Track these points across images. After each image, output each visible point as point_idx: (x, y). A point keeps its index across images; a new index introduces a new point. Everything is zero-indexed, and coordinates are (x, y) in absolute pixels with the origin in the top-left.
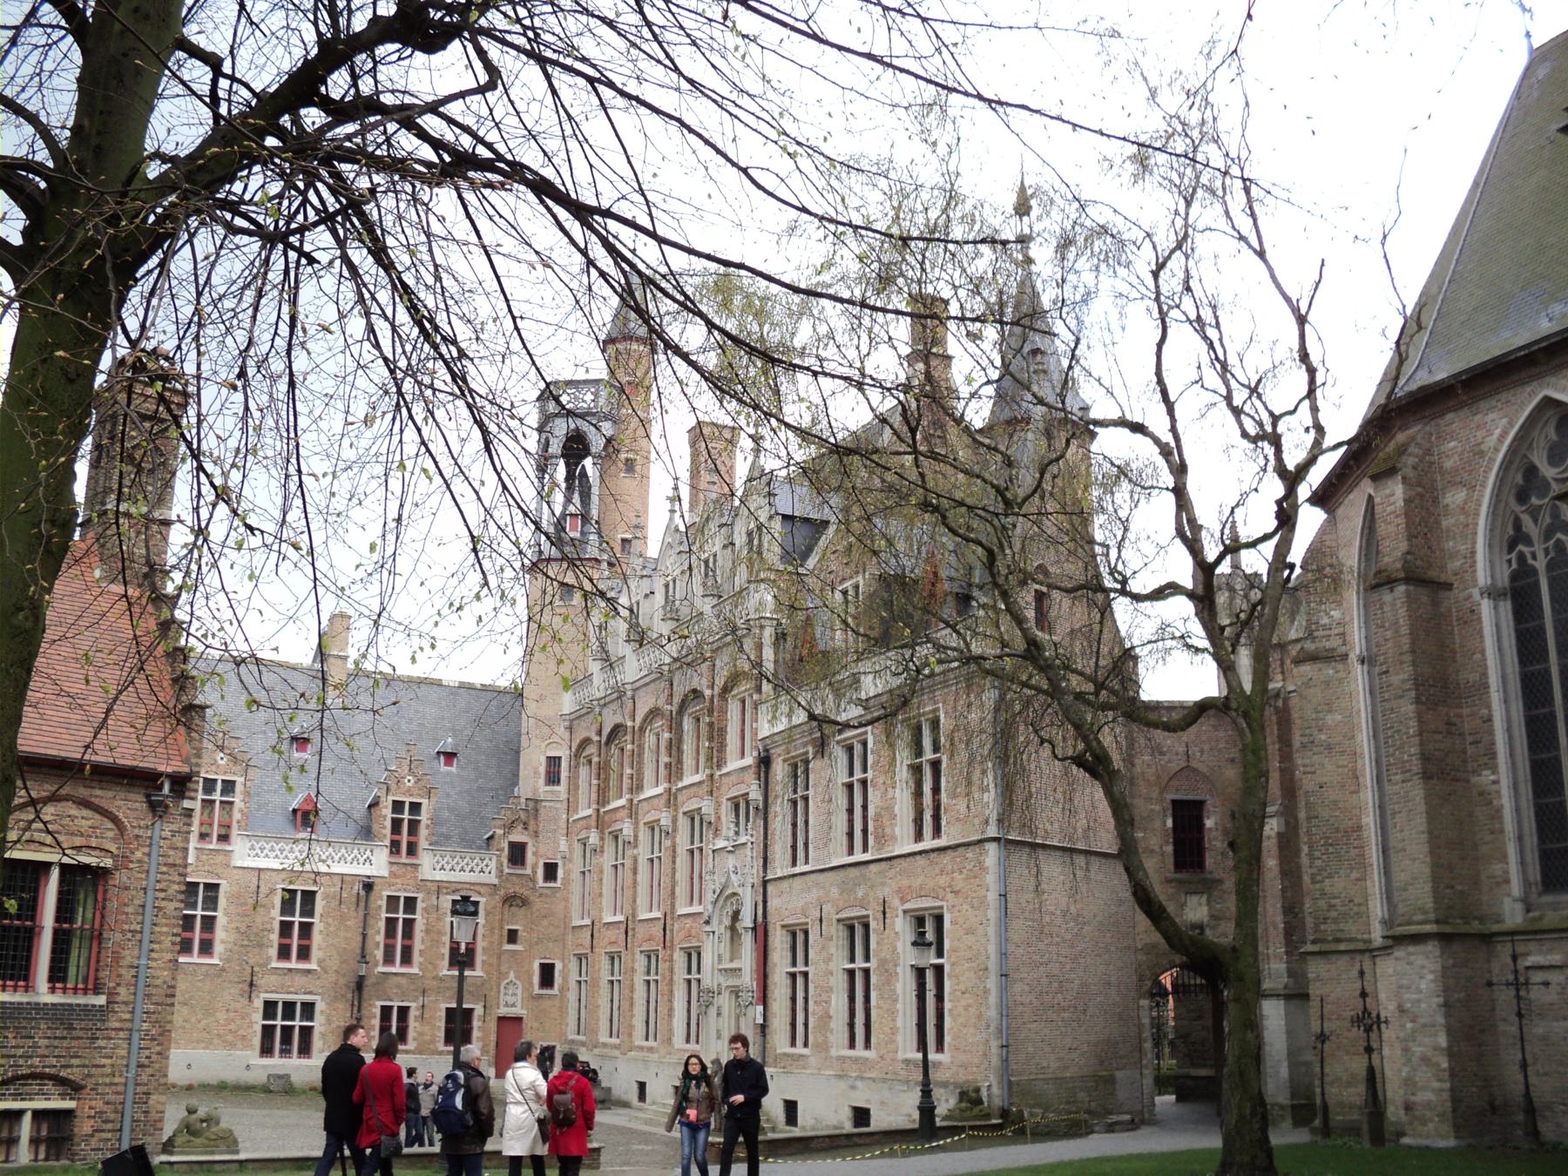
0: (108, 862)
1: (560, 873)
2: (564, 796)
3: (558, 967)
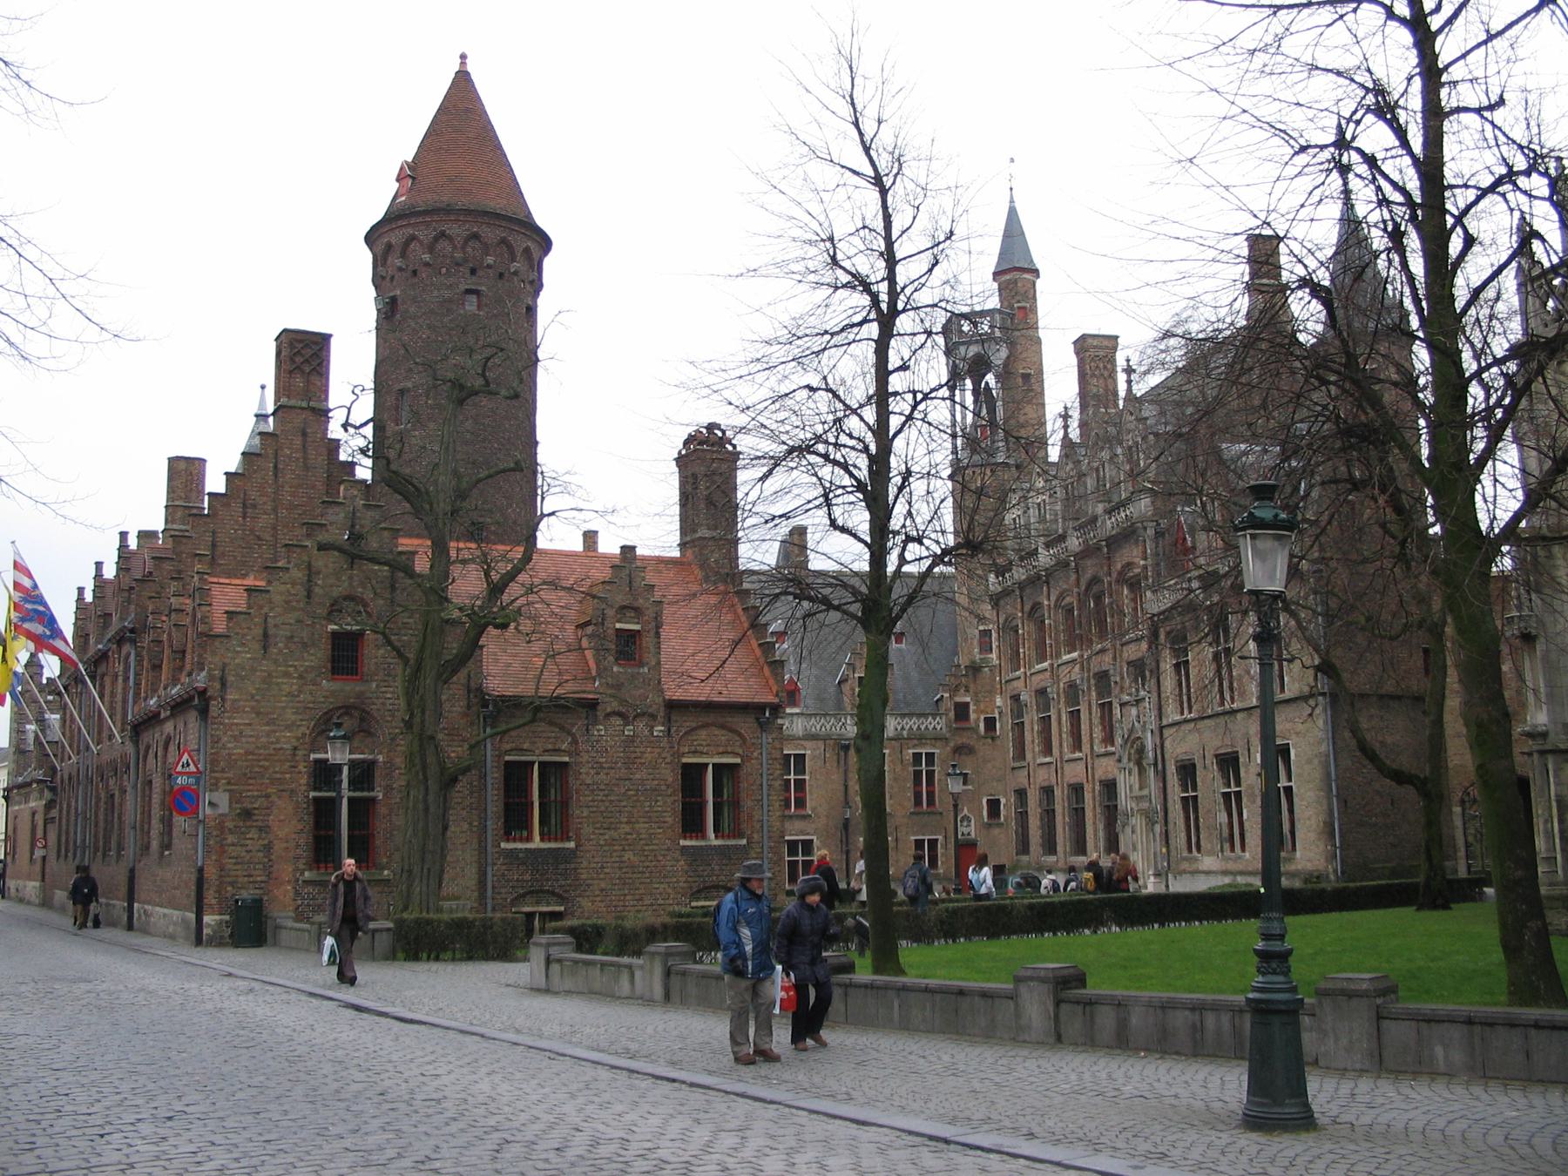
0: (738, 760)
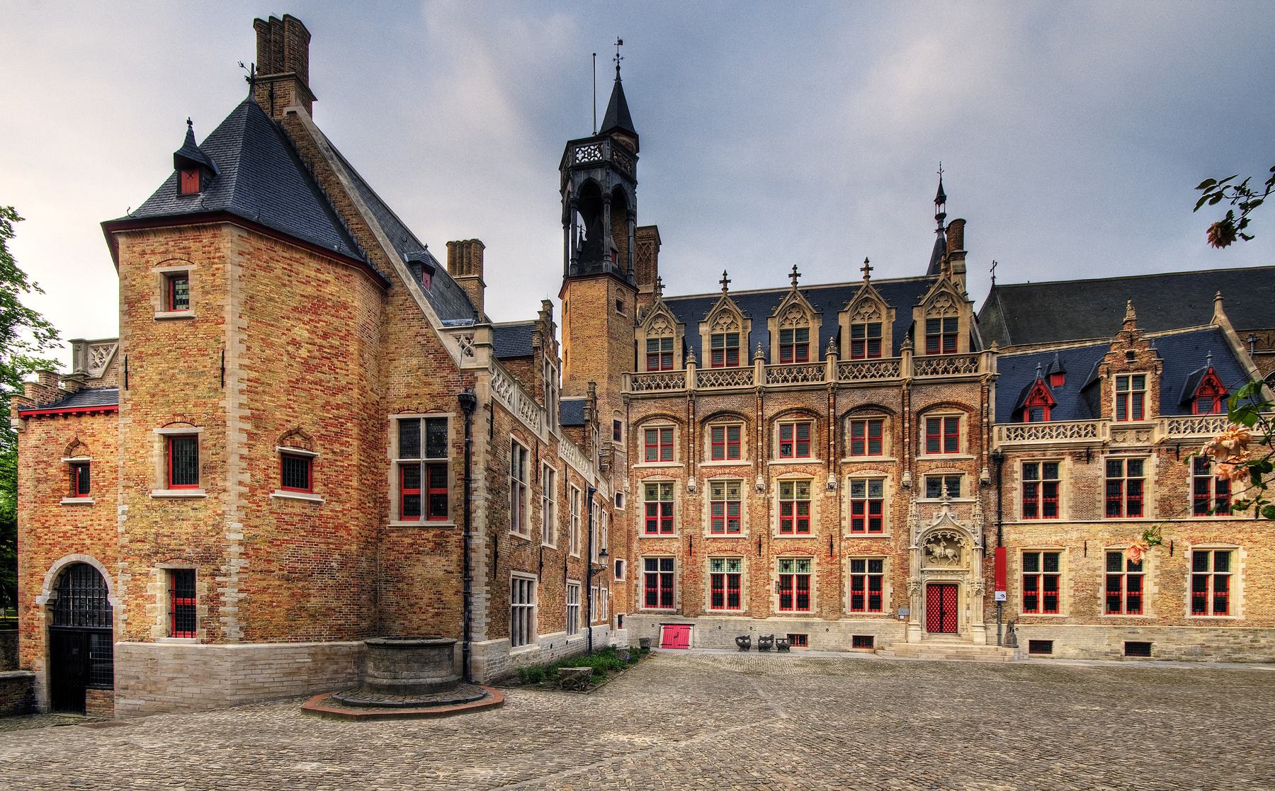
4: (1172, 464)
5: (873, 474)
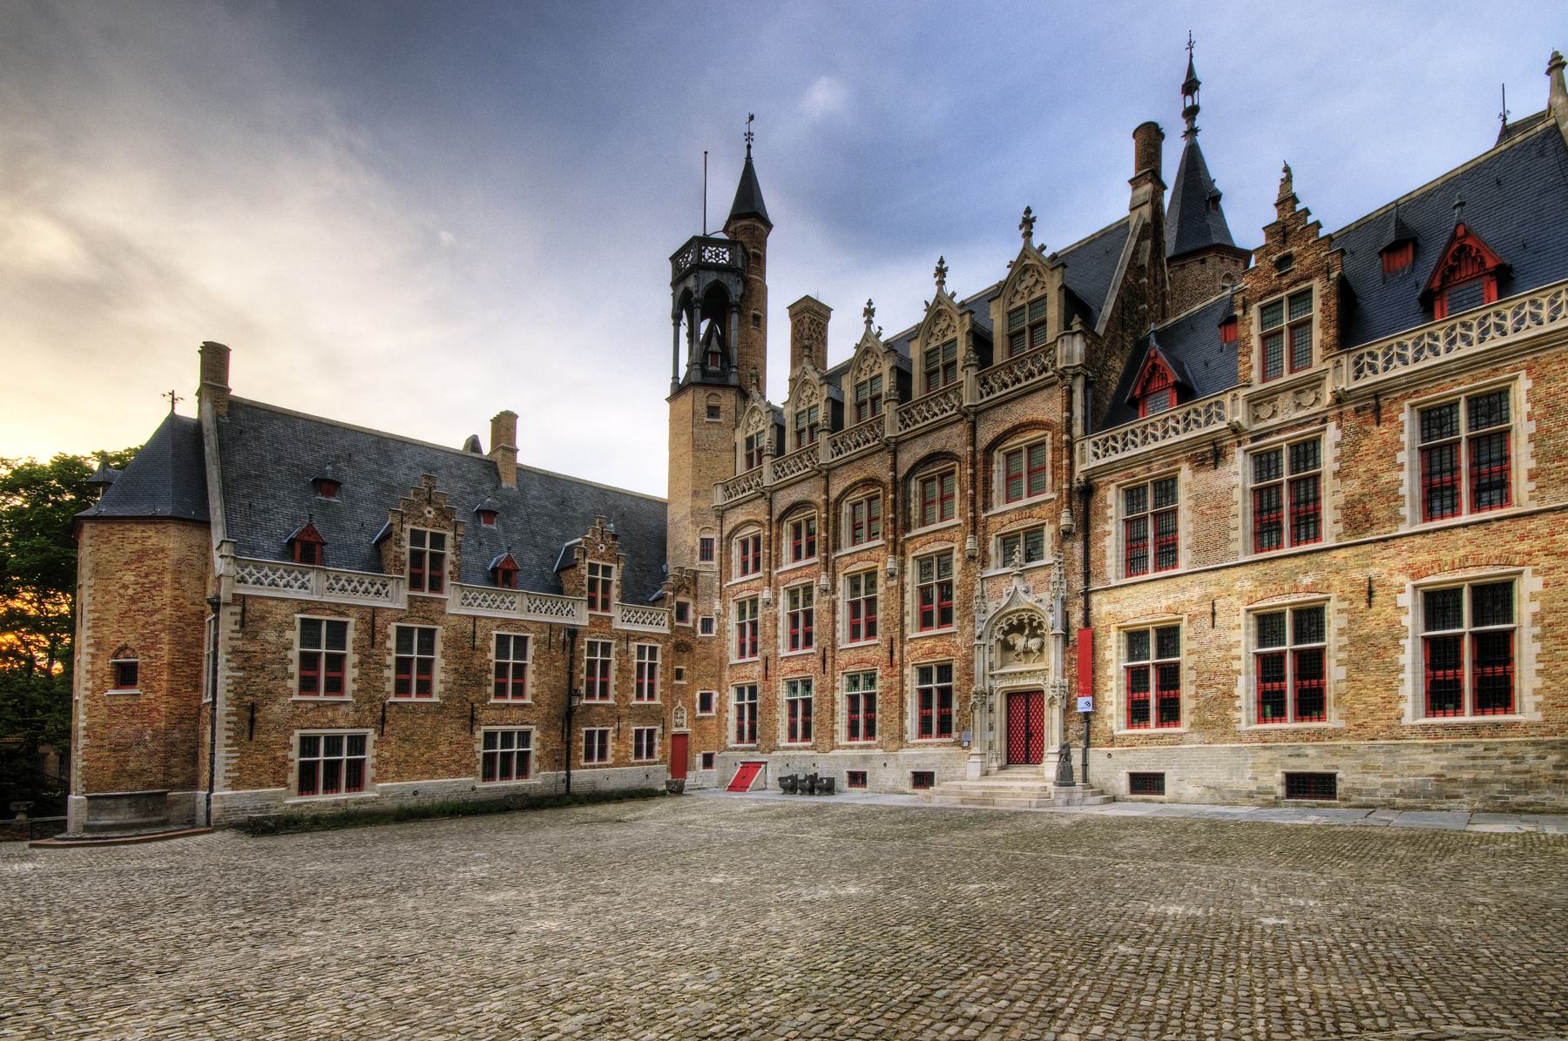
1: (715, 626)
2: (717, 568)
3: (716, 695)
4: (1367, 434)
5: (938, 547)
